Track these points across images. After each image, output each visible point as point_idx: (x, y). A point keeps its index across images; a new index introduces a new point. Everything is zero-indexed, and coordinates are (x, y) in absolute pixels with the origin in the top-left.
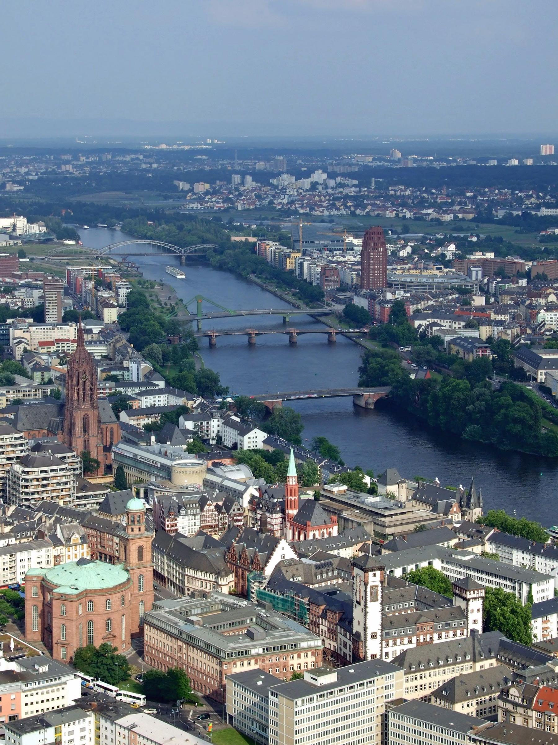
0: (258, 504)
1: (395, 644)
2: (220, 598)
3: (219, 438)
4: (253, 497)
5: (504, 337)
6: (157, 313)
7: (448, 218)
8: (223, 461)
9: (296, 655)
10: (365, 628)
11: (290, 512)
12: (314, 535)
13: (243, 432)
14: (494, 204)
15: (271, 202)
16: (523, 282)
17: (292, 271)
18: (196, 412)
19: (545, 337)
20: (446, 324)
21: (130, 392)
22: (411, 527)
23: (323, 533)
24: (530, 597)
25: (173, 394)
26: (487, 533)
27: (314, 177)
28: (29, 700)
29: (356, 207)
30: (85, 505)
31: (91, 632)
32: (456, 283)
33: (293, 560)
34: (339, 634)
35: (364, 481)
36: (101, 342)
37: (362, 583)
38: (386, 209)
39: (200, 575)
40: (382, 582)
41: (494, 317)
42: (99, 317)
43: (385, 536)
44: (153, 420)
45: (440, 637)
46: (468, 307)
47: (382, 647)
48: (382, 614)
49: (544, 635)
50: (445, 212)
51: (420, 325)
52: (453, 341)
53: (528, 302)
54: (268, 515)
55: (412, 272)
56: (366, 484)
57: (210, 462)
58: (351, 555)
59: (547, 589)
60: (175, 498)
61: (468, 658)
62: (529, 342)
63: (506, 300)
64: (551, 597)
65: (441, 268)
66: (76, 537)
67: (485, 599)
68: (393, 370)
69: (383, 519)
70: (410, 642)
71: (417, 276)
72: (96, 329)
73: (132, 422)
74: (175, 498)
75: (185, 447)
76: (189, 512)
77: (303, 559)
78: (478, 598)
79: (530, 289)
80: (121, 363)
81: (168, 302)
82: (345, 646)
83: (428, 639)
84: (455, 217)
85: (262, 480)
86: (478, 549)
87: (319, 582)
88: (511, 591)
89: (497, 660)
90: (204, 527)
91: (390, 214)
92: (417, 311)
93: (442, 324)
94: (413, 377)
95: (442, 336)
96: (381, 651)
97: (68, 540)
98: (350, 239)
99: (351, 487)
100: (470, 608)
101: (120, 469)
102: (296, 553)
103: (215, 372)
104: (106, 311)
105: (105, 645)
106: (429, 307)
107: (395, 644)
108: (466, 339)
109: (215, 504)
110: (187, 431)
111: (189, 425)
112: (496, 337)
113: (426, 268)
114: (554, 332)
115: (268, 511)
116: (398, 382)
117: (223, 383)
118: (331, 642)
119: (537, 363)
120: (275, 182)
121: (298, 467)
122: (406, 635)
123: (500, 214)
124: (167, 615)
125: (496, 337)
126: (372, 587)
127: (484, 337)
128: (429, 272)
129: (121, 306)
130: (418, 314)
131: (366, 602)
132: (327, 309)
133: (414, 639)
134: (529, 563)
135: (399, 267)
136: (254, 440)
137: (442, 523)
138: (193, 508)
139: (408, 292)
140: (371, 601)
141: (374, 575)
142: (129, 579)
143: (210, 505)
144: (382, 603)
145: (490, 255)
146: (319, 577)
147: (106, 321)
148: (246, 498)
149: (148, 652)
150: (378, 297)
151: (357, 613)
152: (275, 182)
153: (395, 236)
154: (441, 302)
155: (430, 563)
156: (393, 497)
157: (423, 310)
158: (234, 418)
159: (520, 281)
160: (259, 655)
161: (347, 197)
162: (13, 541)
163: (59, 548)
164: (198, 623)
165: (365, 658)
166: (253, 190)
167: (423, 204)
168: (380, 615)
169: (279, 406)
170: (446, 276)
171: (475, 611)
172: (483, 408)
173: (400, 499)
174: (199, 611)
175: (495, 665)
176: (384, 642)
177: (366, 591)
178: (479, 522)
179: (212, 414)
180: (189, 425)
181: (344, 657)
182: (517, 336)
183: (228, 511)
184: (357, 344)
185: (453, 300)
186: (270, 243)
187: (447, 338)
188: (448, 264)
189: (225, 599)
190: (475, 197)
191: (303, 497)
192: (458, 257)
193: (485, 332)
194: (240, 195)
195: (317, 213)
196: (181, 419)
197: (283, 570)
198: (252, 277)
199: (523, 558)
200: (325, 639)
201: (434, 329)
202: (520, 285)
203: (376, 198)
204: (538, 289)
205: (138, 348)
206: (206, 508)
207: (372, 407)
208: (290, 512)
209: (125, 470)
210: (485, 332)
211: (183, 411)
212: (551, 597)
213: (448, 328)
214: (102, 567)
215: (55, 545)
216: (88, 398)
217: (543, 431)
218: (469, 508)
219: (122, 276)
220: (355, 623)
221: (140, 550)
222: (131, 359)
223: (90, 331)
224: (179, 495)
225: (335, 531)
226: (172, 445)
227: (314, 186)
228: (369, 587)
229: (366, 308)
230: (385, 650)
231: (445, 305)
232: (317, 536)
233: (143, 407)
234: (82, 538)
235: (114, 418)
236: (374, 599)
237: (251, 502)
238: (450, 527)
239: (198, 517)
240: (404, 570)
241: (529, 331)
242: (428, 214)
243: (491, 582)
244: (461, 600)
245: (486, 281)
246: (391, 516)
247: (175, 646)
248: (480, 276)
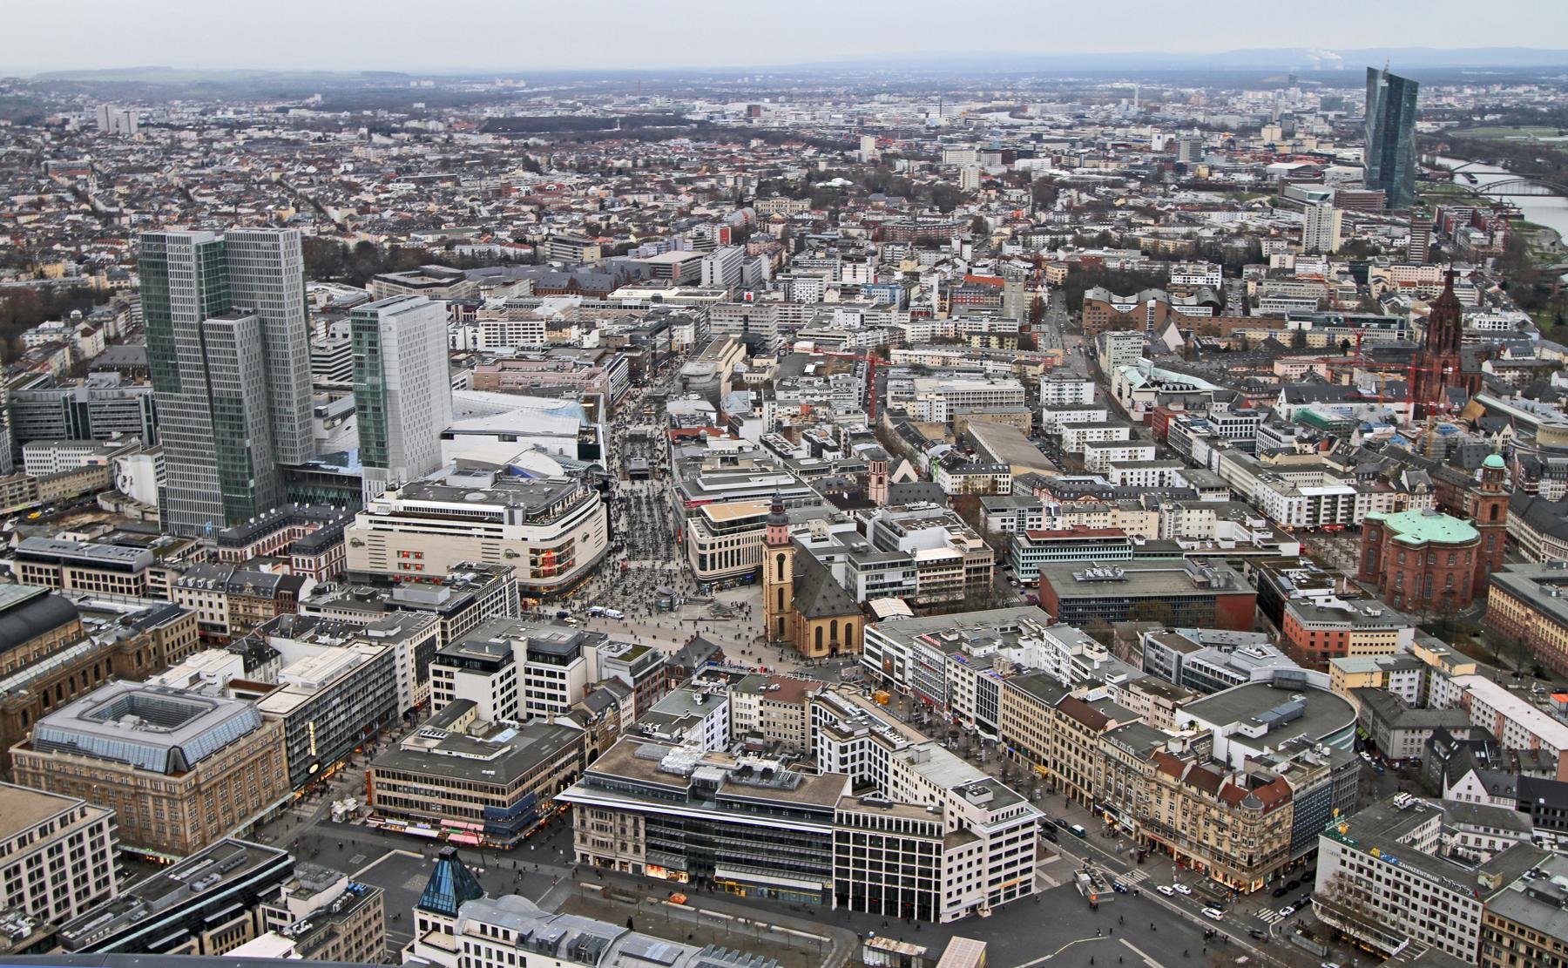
28: (1358, 640)
97: (1413, 487)
214: (1449, 520)
215: (1398, 492)
223: (1458, 274)
234: (1429, 487)
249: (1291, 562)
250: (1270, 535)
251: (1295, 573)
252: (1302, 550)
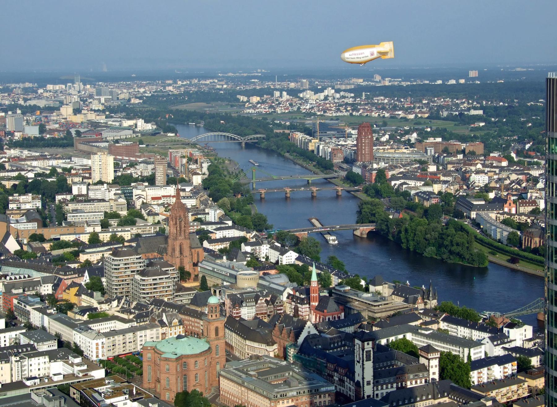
0: (292, 299)
1: (382, 389)
2: (269, 360)
3: (267, 258)
4: (289, 295)
5: (449, 191)
6: (227, 179)
7: (412, 117)
8: (269, 271)
9: (318, 396)
10: (363, 378)
11: (314, 304)
12: (329, 319)
13: (282, 253)
14: (440, 108)
15: (299, 108)
16: (460, 157)
17: (313, 151)
18: (252, 240)
19: (476, 191)
20: (412, 183)
21: (210, 228)
22: (392, 313)
23: (335, 317)
24: (469, 357)
25: (237, 229)
26: (441, 316)
27: (326, 92)
29: (353, 110)
30: (181, 301)
31: (185, 382)
32: (418, 157)
33: (315, 334)
34: (346, 382)
35: (361, 283)
36: (191, 197)
37: (361, 349)
38: (372, 111)
39: (256, 345)
40: (373, 348)
41: (442, 178)
42: (189, 182)
43: (375, 319)
44: (225, 246)
45: (411, 384)
46: (426, 172)
47: (374, 390)
48: (374, 369)
49: (478, 381)
50: (410, 113)
51: (395, 184)
52: (417, 194)
53: (464, 169)
54: (299, 305)
55: (389, 151)
56: (362, 285)
57: (261, 272)
58: (353, 331)
59: (481, 352)
60: (239, 296)
61: (430, 397)
62: (465, 194)
63: (450, 167)
64: (483, 357)
65: (408, 148)
66: (176, 321)
67: (440, 359)
68: (379, 213)
69: (373, 308)
70: (392, 387)
71: (392, 153)
72: (188, 189)
73: (211, 248)
74: (239, 296)
75: (245, 263)
76: (248, 304)
77: (322, 334)
78: (436, 358)
79: (465, 161)
80: (204, 210)
81: (234, 172)
82: (350, 390)
83: (404, 385)
84: (416, 116)
85: (295, 284)
86: (435, 327)
87: (333, 349)
88: (457, 353)
89: (449, 398)
90: (257, 314)
91: (375, 114)
92: (393, 175)
93: (409, 183)
94: (391, 217)
95: (409, 191)
96: (374, 393)
97: (170, 323)
98: (349, 130)
99: (352, 287)
100: (431, 365)
101: (204, 278)
102: (317, 330)
103: (264, 215)
104: (195, 177)
105: (195, 390)
106: (401, 173)
107: (382, 389)
108: (424, 193)
109: (265, 299)
110: (246, 253)
111: (248, 249)
112: (444, 191)
113: (398, 148)
114: (481, 188)
115: (299, 303)
116: (382, 220)
117: (269, 222)
118: (341, 388)
119: (472, 207)
120: (301, 95)
121: (318, 275)
122: (390, 383)
123: (445, 114)
124: (234, 371)
125: (444, 191)
126: (367, 352)
127: (436, 192)
128: (400, 151)
129: (204, 174)
130: (394, 178)
131: (363, 361)
132: (335, 175)
133: (395, 385)
134: (468, 335)
135: (381, 148)
136: (290, 258)
137: (411, 310)
138: (250, 302)
139: (387, 163)
140: (366, 361)
141: (368, 344)
142: (210, 348)
143: (262, 300)
144: (373, 362)
145: (439, 140)
146: (332, 346)
147: (195, 184)
148: (285, 295)
149: (222, 395)
150: (368, 166)
151: (358, 368)
152: (301, 95)
153: (378, 128)
154: (408, 169)
155: (404, 336)
156: (379, 294)
157: (397, 174)
158: (276, 244)
159: (458, 156)
160: (294, 396)
161: (347, 104)
162: (135, 324)
163: (164, 328)
164: (254, 376)
165: (364, 397)
166: (287, 100)
167: (395, 108)
168: (372, 370)
169: (306, 236)
170: (412, 153)
171: (434, 367)
172: (437, 236)
173: (384, 295)
174: (255, 368)
175: (447, 402)
176: (375, 387)
177: (363, 354)
178: (435, 309)
179: (262, 242)
180: (248, 249)
181: (349, 397)
182: (457, 191)
183: (273, 304)
184: (355, 197)
185: (416, 168)
186: (299, 133)
187: (413, 192)
188: (412, 146)
189: (272, 360)
190: (428, 103)
191: (321, 294)
192: (419, 141)
193: (436, 188)
194: (280, 104)
195: (328, 114)
196: (243, 245)
197: (309, 341)
198: (287, 155)
199: (464, 332)
200: (337, 386)
201: (404, 186)
202: (458, 158)
203: (366, 104)
204: (470, 161)
205: (215, 200)
206: (259, 302)
207: (365, 236)
208: (314, 304)
209: (207, 278)
210: (436, 188)
211: (244, 240)
212: (483, 357)
213: (413, 185)
214: (193, 340)
215: (162, 327)
216: (183, 233)
217: (476, 251)
218: (429, 300)
219: (204, 156)
220: (356, 375)
221: (217, 329)
222: (210, 207)
223: (184, 190)
224: (241, 294)
225: (342, 316)
226: (237, 261)
227: (326, 98)
228: (365, 351)
229: (360, 174)
230: (376, 392)
231: (411, 171)
232: (331, 319)
233: (218, 238)
234: (180, 321)
235: (199, 245)
236: (368, 359)
237: (288, 298)
238: (416, 312)
239: (253, 307)
240: (388, 340)
241: (465, 187)
242: (399, 115)
243: (444, 348)
244: (425, 359)
245: (436, 155)
246: (379, 306)
247: (240, 391)
248: (433, 153)
249: (100, 382)
250: (85, 367)
251: (102, 389)
252: (107, 374)
